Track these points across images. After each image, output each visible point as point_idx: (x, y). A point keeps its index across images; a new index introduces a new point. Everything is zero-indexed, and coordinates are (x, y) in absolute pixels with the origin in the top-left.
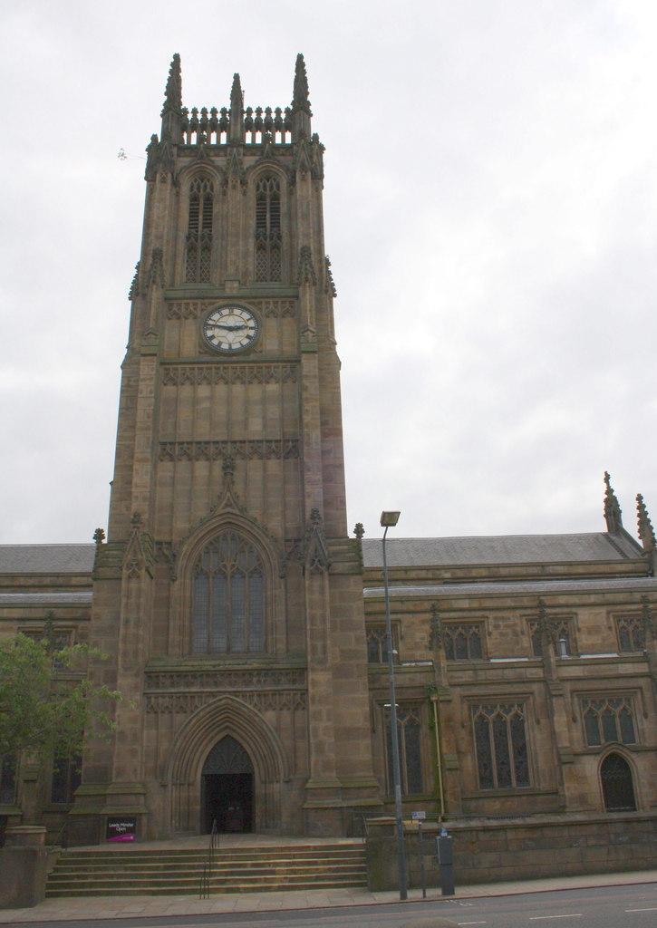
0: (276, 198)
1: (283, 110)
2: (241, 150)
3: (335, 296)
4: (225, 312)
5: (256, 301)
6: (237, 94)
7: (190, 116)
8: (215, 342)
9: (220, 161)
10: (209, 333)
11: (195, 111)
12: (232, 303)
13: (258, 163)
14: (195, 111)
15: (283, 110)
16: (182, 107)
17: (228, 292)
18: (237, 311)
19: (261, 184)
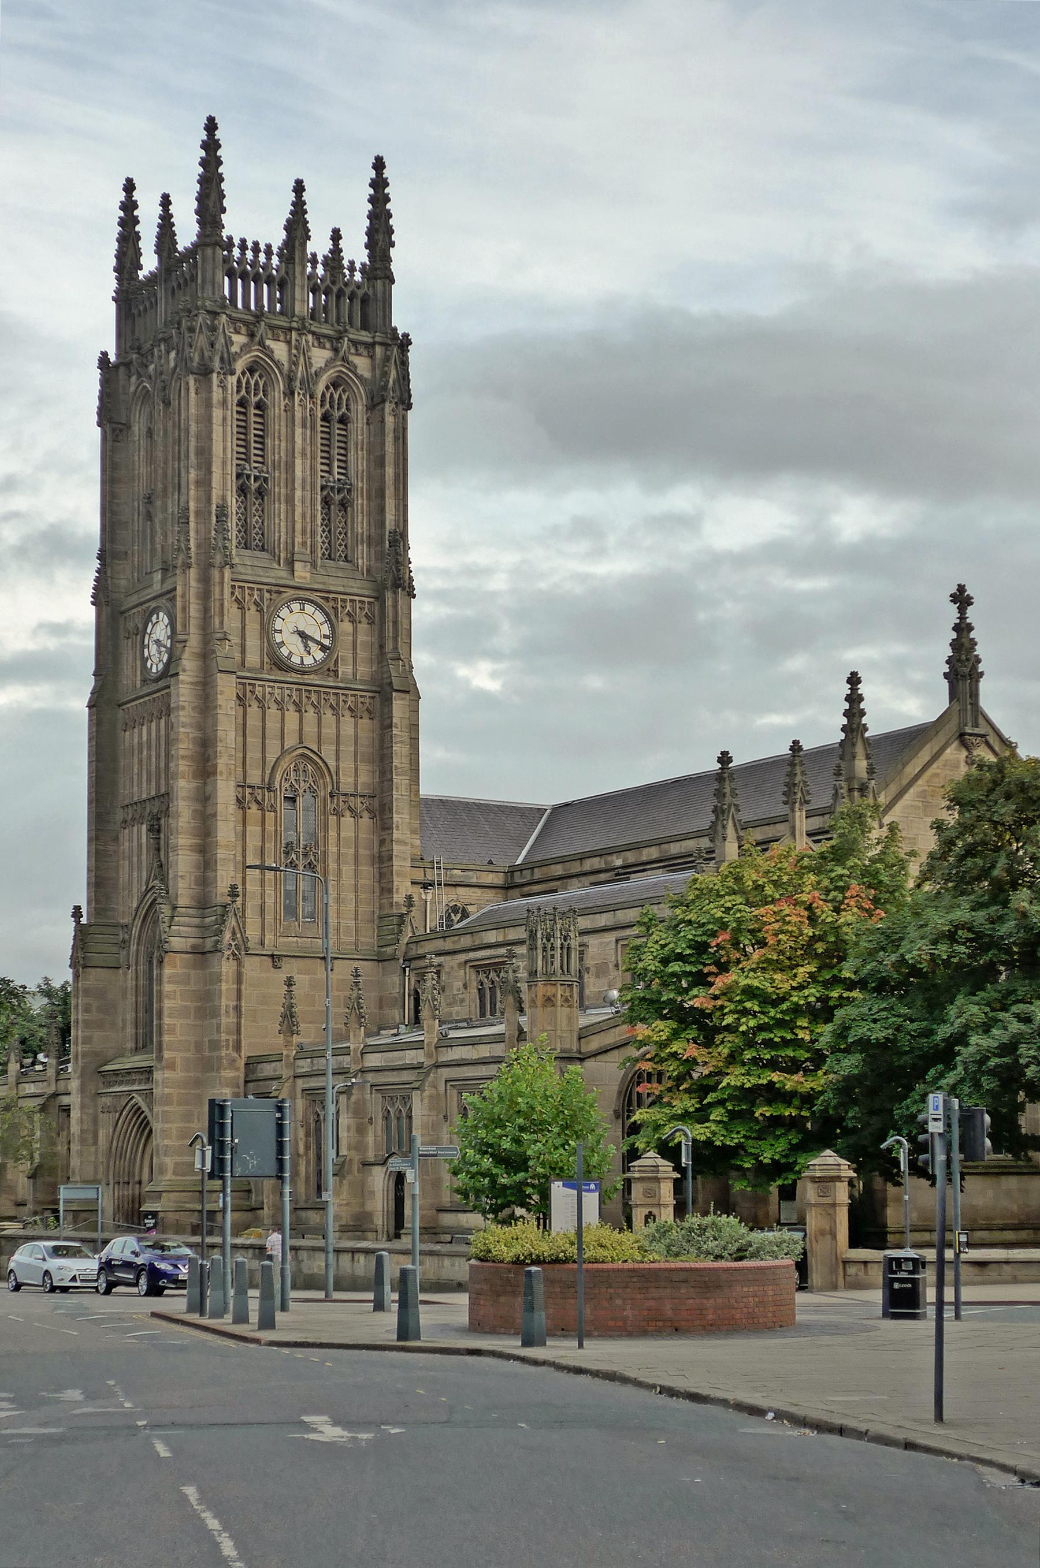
0: (343, 420)
1: (358, 266)
2: (310, 337)
3: (414, 596)
4: (296, 606)
5: (331, 596)
6: (297, 225)
7: (236, 252)
8: (284, 651)
9: (280, 350)
10: (278, 638)
11: (243, 246)
12: (303, 595)
13: (329, 364)
14: (243, 246)
15: (358, 266)
16: (225, 234)
17: (297, 581)
18: (309, 608)
19: (328, 396)
